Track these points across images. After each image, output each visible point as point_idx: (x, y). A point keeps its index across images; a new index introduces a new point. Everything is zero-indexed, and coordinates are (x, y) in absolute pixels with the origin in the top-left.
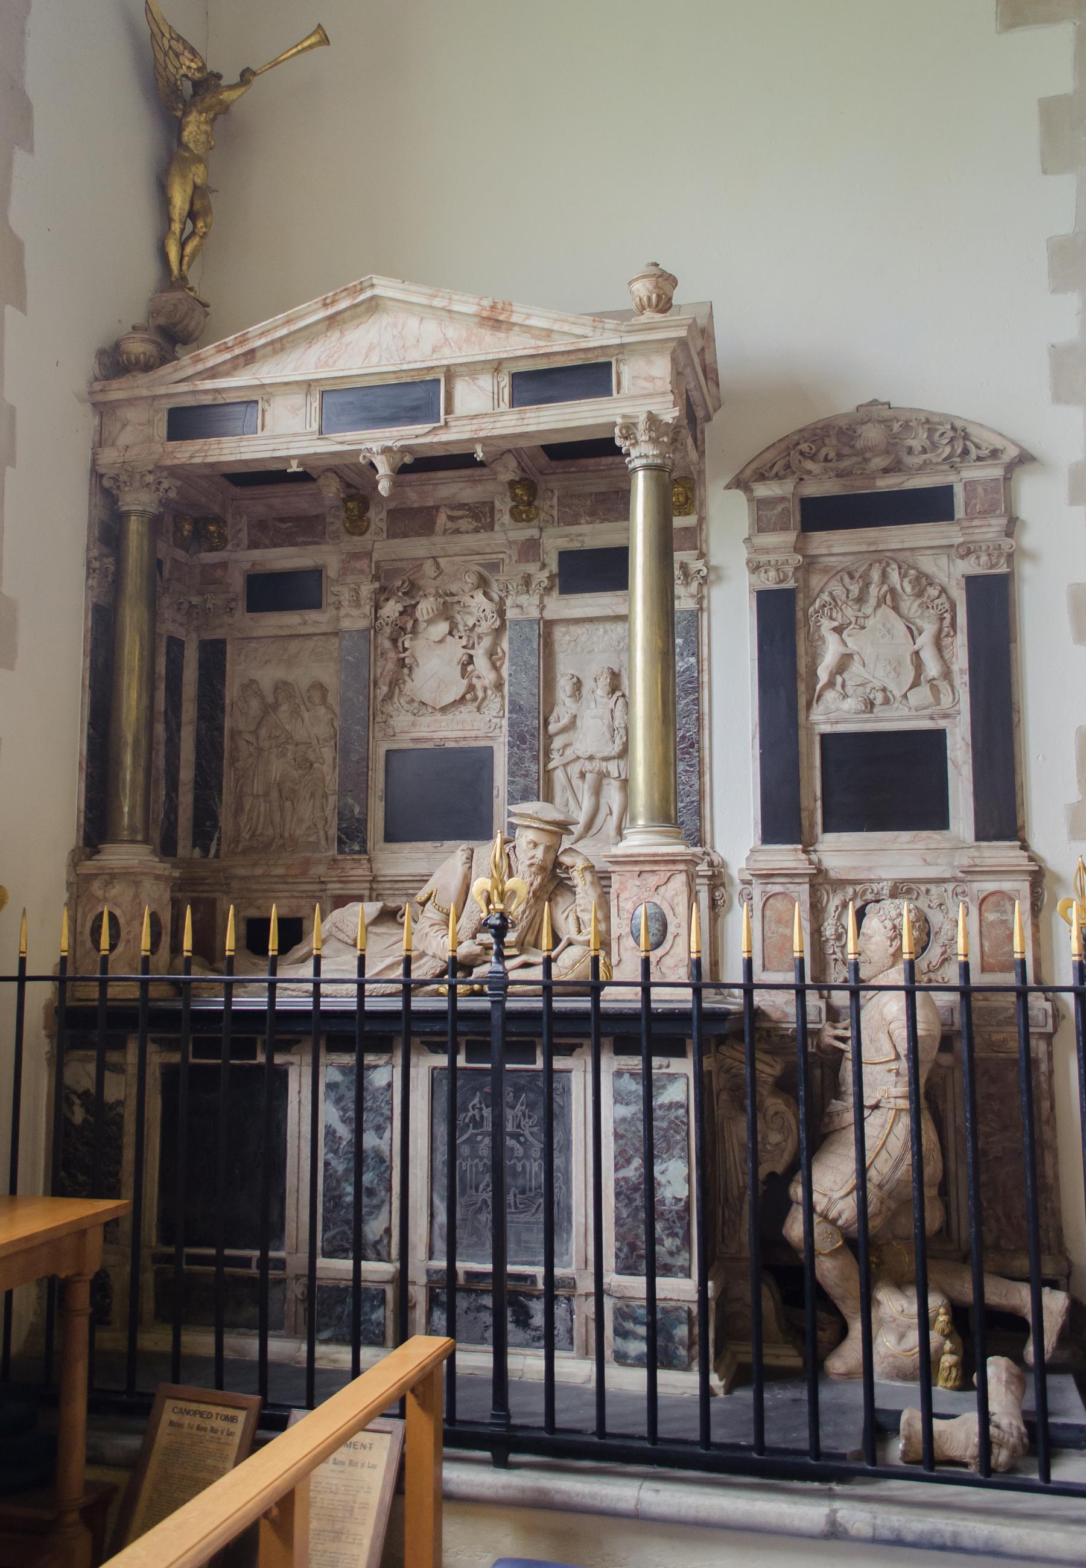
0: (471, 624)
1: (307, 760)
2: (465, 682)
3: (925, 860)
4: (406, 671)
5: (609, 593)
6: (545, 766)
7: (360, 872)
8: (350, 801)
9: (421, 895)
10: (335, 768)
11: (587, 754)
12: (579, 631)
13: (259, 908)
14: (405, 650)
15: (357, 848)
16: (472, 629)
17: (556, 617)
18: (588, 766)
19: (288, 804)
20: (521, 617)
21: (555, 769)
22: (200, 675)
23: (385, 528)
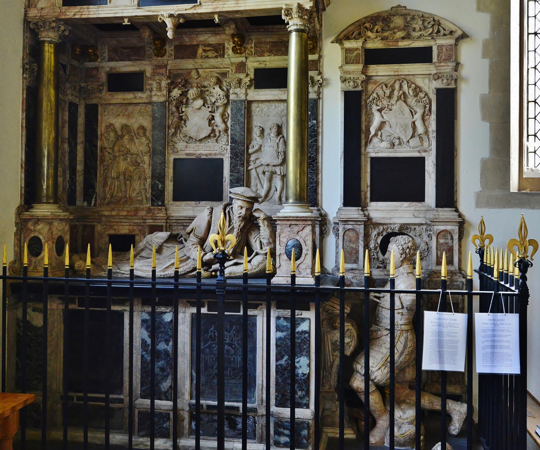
0: (213, 101)
1: (136, 162)
2: (211, 128)
3: (414, 215)
4: (183, 122)
6: (247, 168)
8: (157, 182)
9: (189, 229)
10: (150, 166)
11: (266, 164)
12: (264, 107)
13: (115, 230)
14: (183, 112)
15: (160, 203)
16: (214, 103)
17: (253, 99)
18: (266, 169)
19: (128, 182)
20: (236, 99)
22: (86, 121)
23: (173, 54)
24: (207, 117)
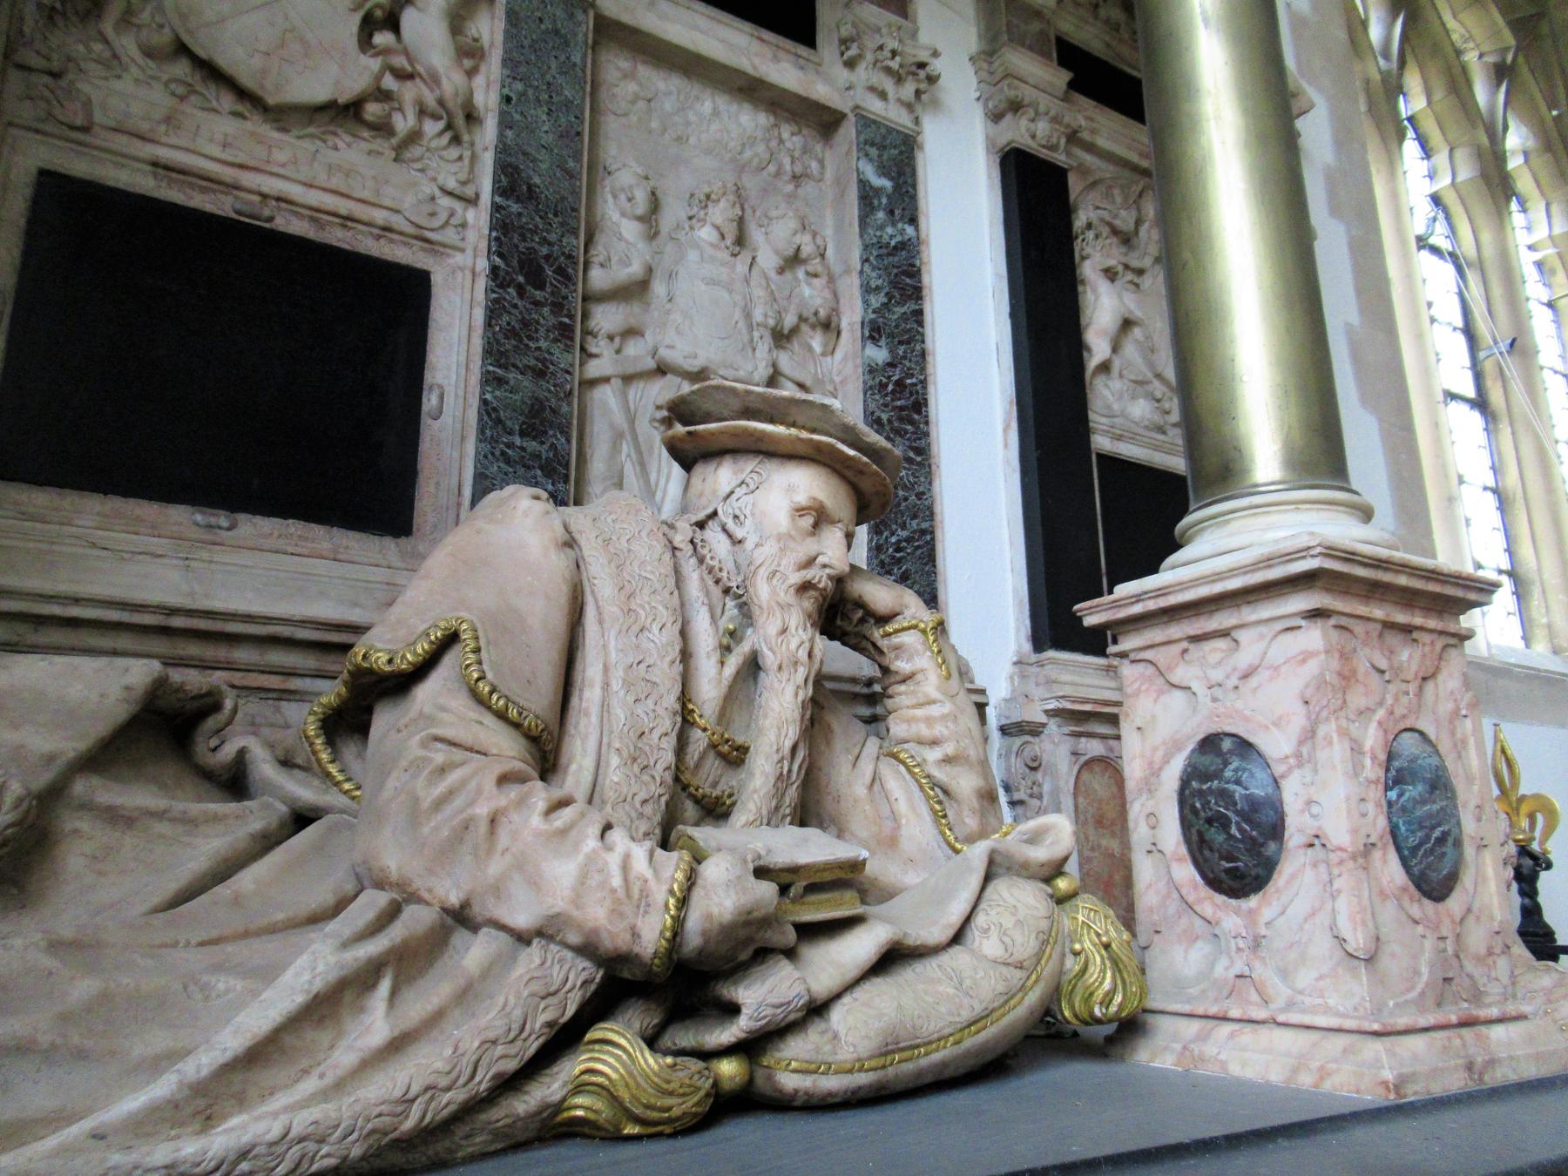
5: (747, 27)
11: (693, 365)
12: (661, 85)
21: (593, 383)
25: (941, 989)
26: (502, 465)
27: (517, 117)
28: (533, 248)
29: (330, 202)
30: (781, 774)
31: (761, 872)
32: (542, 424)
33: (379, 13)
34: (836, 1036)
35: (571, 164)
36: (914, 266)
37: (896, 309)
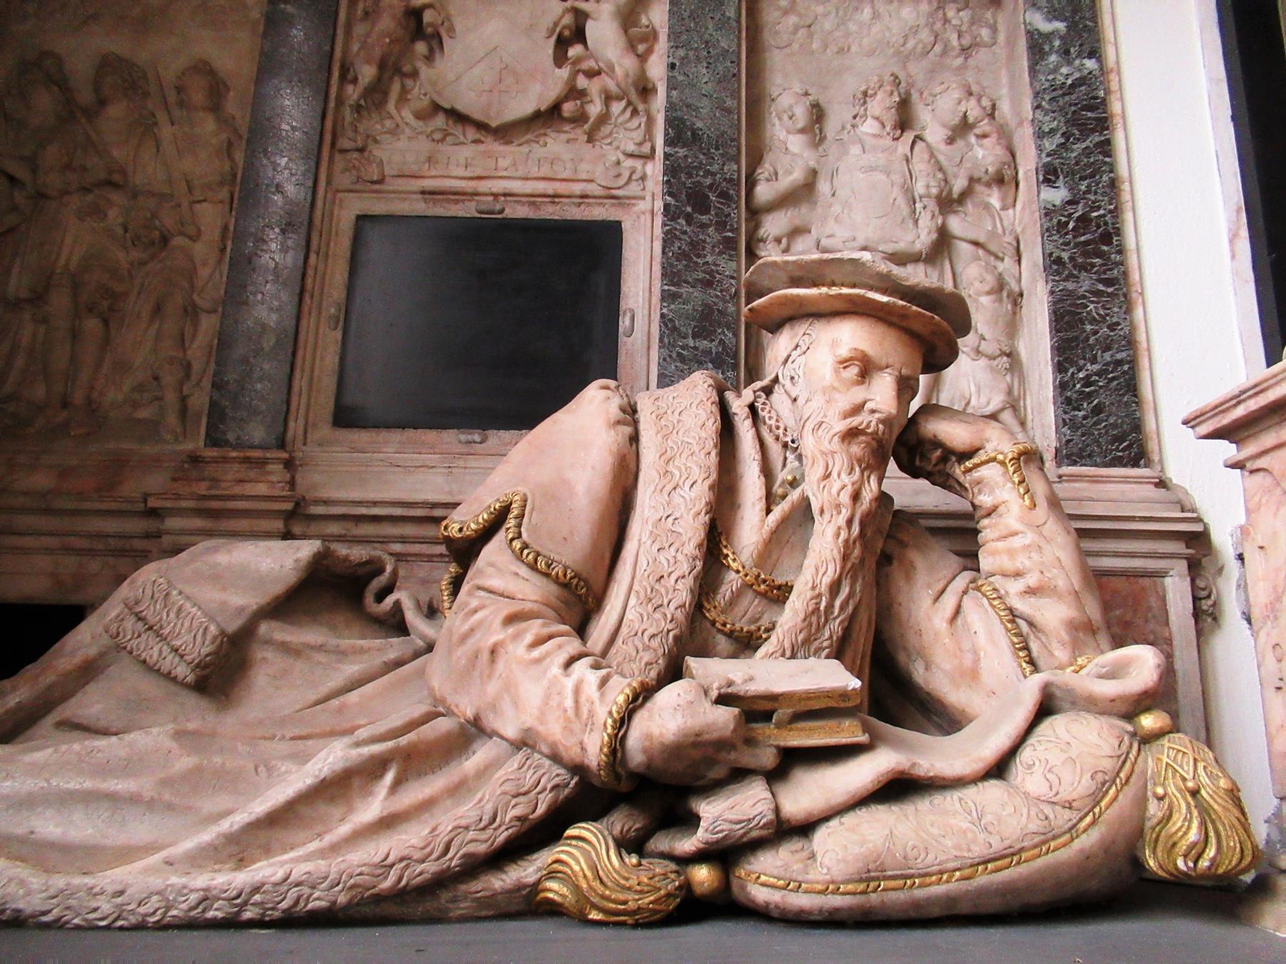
2: (564, 73)
4: (421, 47)
7: (262, 489)
24: (547, 22)
25: (952, 821)
26: (678, 364)
27: (681, 78)
28: (698, 182)
29: (541, 187)
30: (819, 608)
31: (724, 699)
32: (711, 325)
33: (567, 33)
34: (813, 856)
35: (729, 103)
36: (1097, 98)
37: (1075, 147)
